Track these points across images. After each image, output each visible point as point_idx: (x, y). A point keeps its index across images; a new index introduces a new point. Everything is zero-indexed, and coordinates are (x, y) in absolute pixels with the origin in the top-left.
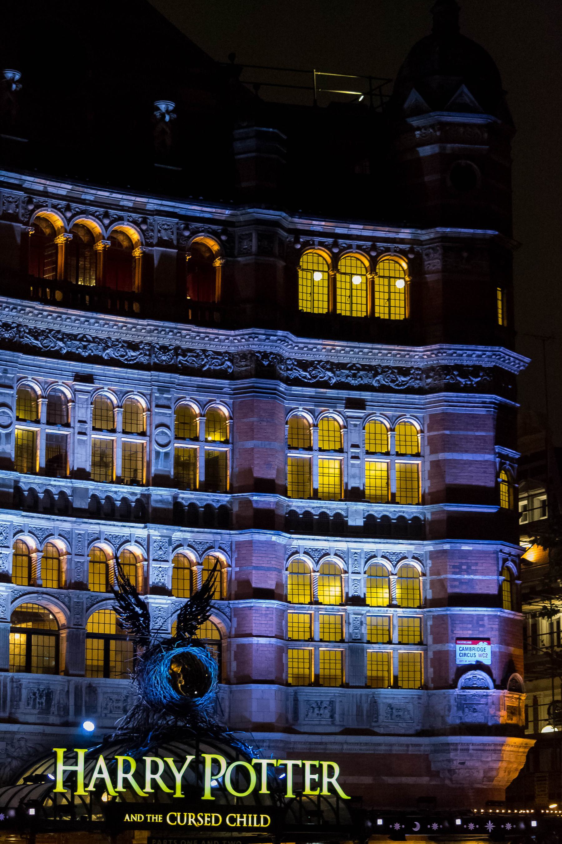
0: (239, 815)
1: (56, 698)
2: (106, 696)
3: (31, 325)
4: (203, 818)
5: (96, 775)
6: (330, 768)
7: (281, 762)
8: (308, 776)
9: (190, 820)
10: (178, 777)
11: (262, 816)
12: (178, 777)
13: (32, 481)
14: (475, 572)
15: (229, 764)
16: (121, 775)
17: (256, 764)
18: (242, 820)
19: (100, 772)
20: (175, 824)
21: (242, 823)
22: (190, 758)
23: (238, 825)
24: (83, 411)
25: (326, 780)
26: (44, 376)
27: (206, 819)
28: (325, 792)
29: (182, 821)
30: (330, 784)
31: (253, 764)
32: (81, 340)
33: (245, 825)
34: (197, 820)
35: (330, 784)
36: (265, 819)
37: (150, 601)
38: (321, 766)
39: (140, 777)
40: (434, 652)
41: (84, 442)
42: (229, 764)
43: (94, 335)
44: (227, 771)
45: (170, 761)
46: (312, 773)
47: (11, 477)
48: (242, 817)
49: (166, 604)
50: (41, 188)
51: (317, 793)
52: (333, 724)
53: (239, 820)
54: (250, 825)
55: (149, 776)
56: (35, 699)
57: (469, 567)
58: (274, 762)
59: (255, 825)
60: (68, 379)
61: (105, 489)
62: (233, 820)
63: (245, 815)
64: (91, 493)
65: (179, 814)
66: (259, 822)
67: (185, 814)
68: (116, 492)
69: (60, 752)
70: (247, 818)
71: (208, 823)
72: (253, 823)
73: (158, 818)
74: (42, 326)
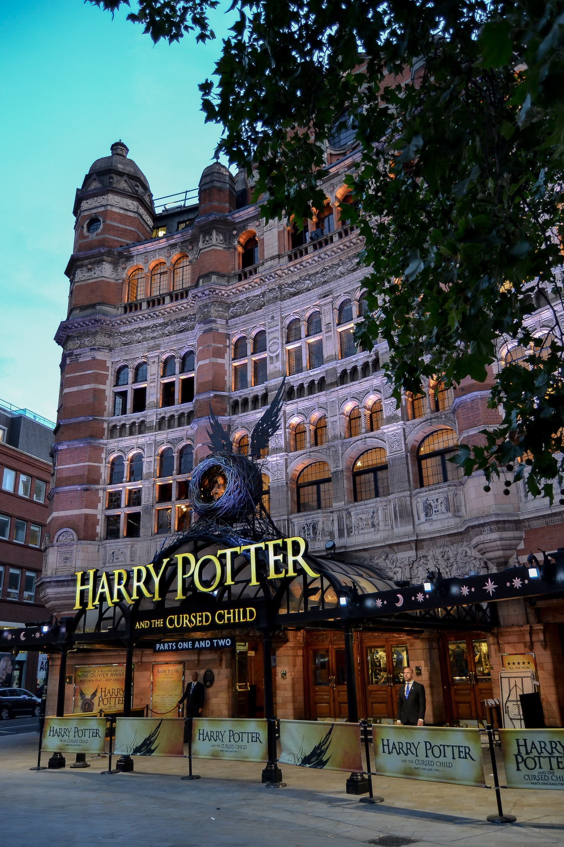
0: (226, 611)
1: (320, 526)
2: (358, 516)
3: (290, 282)
4: (195, 618)
5: (100, 590)
6: (296, 545)
8: (272, 558)
10: (157, 580)
11: (248, 609)
12: (157, 580)
15: (197, 561)
16: (116, 587)
19: (103, 587)
21: (229, 619)
22: (165, 561)
23: (226, 622)
25: (291, 559)
27: (198, 619)
28: (291, 573)
29: (178, 624)
30: (295, 562)
32: (322, 271)
33: (232, 621)
34: (190, 621)
35: (295, 562)
36: (251, 612)
37: (386, 431)
38: (285, 544)
39: (128, 586)
42: (197, 561)
44: (194, 568)
45: (151, 567)
46: (275, 554)
48: (229, 613)
49: (398, 429)
51: (282, 575)
53: (226, 616)
54: (237, 621)
55: (136, 584)
56: (305, 532)
58: (237, 549)
59: (242, 620)
62: (221, 617)
63: (232, 611)
64: (340, 371)
66: (245, 616)
68: (356, 361)
69: (79, 575)
70: (234, 612)
72: (239, 619)
73: (159, 623)
74: (296, 278)
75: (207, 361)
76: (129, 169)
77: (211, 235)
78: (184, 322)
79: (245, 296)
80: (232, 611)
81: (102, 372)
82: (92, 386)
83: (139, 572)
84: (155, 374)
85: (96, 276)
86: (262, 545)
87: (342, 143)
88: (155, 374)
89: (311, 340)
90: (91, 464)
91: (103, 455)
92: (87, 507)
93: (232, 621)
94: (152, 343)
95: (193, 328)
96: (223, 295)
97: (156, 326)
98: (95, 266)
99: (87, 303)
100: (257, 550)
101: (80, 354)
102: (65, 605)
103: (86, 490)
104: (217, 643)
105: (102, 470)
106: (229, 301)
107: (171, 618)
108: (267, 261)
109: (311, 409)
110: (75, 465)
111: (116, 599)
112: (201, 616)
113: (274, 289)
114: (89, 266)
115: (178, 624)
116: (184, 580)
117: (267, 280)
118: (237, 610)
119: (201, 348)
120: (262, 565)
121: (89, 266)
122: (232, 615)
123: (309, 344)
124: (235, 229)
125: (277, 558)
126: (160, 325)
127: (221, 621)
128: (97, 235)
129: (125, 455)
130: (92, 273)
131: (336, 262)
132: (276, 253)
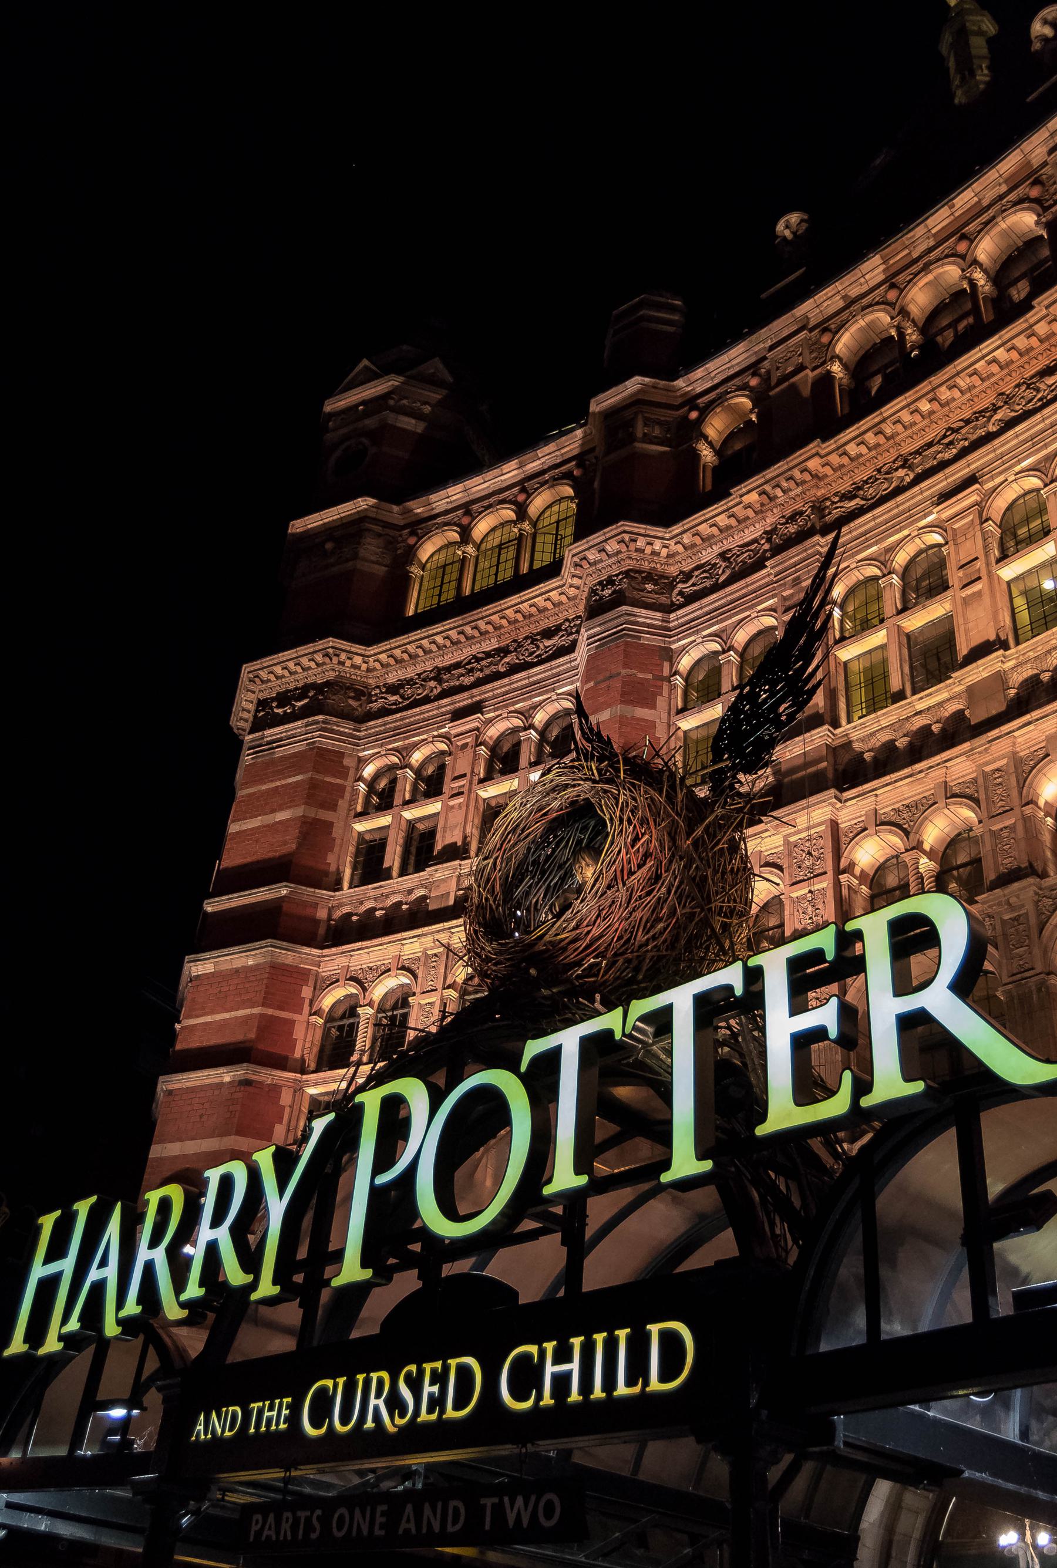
0: (550, 1346)
5: (94, 1275)
7: (641, 1007)
8: (781, 1026)
9: (373, 1401)
11: (654, 1329)
13: (875, 727)
16: (143, 1254)
17: (536, 1060)
18: (568, 1370)
20: (323, 1430)
21: (562, 1382)
23: (547, 1400)
24: (969, 544)
25: (885, 1009)
26: (876, 543)
27: (429, 1389)
28: (890, 1082)
30: (915, 1025)
31: (523, 1068)
33: (575, 1396)
34: (395, 1403)
36: (670, 1340)
41: (979, 594)
43: (967, 415)
47: (818, 742)
48: (563, 1355)
50: (839, 303)
51: (837, 1106)
53: (550, 1369)
54: (598, 1393)
58: (611, 1021)
59: (622, 1389)
60: (925, 516)
61: (1041, 650)
62: (527, 1377)
63: (577, 1342)
64: (1017, 678)
65: (341, 1381)
66: (638, 1370)
67: (361, 1377)
71: (430, 1411)
72: (610, 1383)
78: (549, 638)
79: (717, 549)
80: (577, 1342)
81: (328, 779)
82: (299, 811)
83: (227, 1183)
84: (464, 775)
86: (732, 976)
88: (464, 775)
89: (916, 621)
90: (270, 1012)
91: (306, 992)
92: (239, 1133)
93: (575, 1396)
94: (462, 700)
95: (571, 648)
96: (655, 553)
97: (478, 660)
100: (707, 1007)
103: (247, 1083)
104: (499, 1511)
105: (299, 1033)
106: (673, 570)
107: (323, 1390)
109: (923, 807)
111: (132, 1308)
112: (439, 1378)
113: (801, 513)
115: (344, 1421)
116: (376, 1193)
117: (779, 492)
118: (600, 1338)
119: (592, 684)
120: (731, 1086)
122: (574, 1367)
123: (908, 636)
124: (695, 407)
125: (806, 1021)
126: (488, 655)
127: (525, 1398)
129: (364, 989)
131: (985, 403)
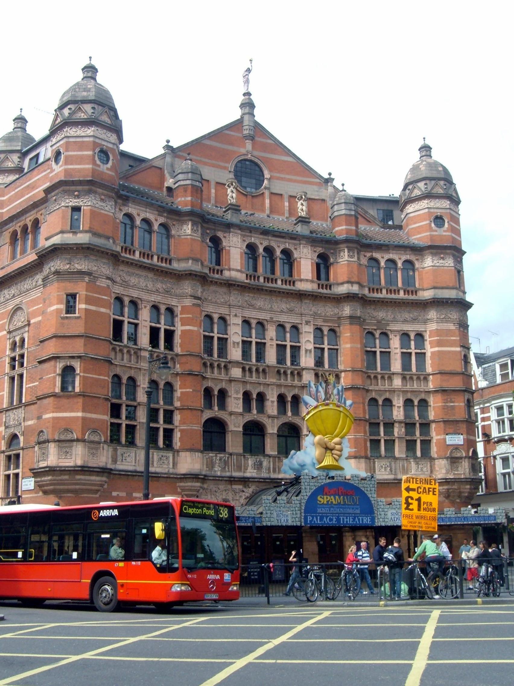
14: (453, 402)
40: (437, 440)
52: (392, 474)
57: (451, 399)
75: (195, 329)
76: (111, 105)
77: (197, 227)
85: (106, 208)
87: (243, 184)
98: (107, 199)
99: (100, 231)
101: (97, 277)
102: (86, 490)
108: (233, 270)
110: (97, 377)
114: (103, 197)
121: (103, 197)
128: (107, 169)
130: (104, 204)
132: (239, 268)
